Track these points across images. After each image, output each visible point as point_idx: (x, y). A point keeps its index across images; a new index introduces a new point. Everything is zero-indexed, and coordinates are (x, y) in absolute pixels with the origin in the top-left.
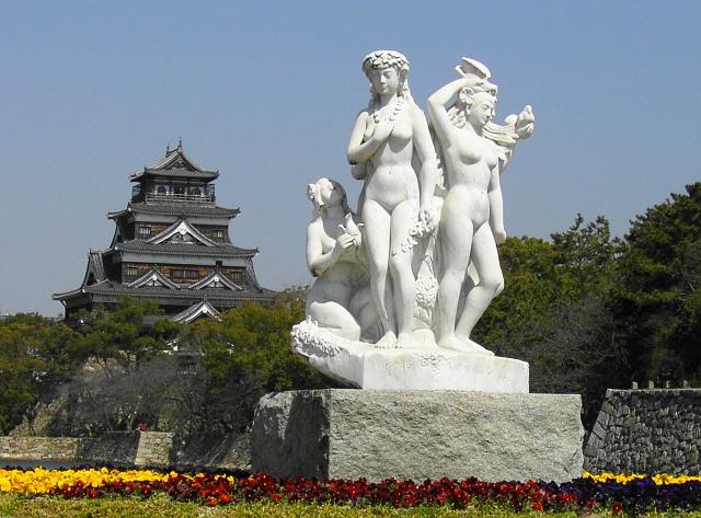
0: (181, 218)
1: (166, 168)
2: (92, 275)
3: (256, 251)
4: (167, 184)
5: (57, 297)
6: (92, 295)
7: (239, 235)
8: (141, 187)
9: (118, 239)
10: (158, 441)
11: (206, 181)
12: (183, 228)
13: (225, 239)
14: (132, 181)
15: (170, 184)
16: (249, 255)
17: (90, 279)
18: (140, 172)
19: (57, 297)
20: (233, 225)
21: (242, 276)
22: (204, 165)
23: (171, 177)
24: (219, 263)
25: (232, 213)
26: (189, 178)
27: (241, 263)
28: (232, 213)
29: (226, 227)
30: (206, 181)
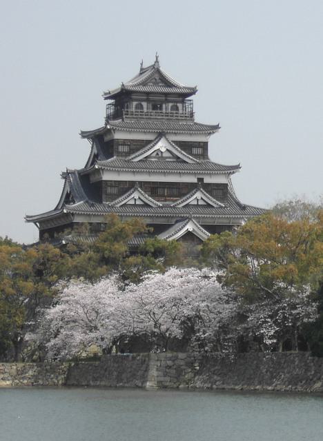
0: (161, 135)
1: (144, 84)
4: (144, 101)
6: (73, 214)
7: (217, 154)
8: (115, 105)
9: (94, 158)
10: (170, 363)
11: (184, 96)
12: (162, 145)
13: (204, 155)
14: (106, 99)
15: (148, 100)
18: (115, 87)
19: (29, 219)
20: (213, 141)
22: (180, 77)
23: (148, 94)
24: (201, 180)
26: (166, 94)
29: (204, 146)
30: (184, 96)
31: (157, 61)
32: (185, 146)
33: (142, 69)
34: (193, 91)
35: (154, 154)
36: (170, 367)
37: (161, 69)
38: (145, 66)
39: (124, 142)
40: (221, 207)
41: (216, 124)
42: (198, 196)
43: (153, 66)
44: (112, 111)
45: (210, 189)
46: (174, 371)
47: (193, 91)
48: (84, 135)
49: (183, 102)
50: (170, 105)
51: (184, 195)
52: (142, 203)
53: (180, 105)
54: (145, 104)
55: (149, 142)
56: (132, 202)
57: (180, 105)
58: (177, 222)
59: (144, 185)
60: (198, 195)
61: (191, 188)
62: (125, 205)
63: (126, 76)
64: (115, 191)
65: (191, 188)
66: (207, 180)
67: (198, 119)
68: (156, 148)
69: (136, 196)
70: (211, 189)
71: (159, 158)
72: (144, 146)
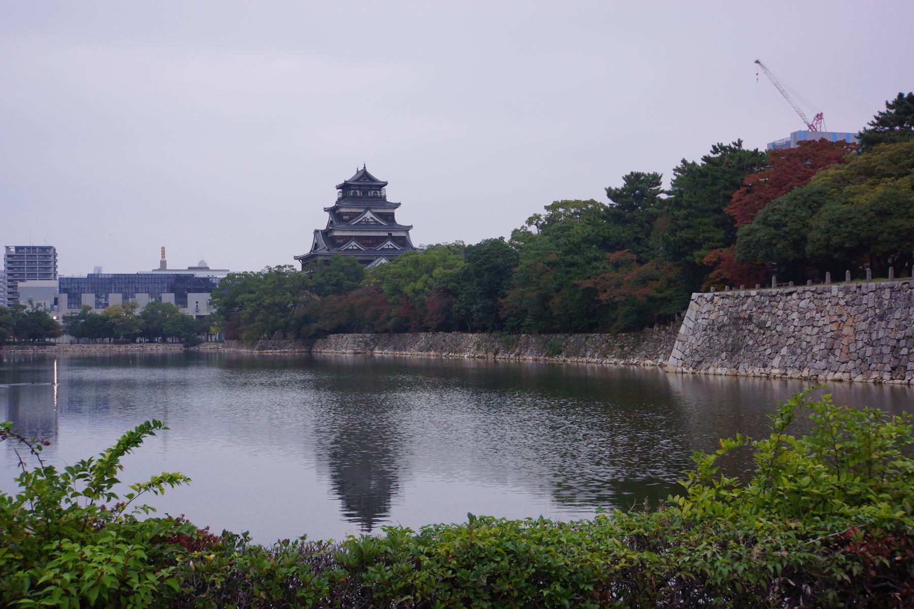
0: (367, 209)
1: (358, 180)
2: (316, 244)
3: (411, 227)
5: (296, 258)
7: (401, 218)
9: (331, 223)
10: (361, 339)
12: (369, 215)
13: (393, 220)
14: (337, 189)
16: (407, 229)
17: (316, 246)
19: (296, 258)
21: (404, 242)
23: (360, 186)
24: (390, 234)
25: (397, 205)
26: (370, 186)
27: (403, 234)
28: (397, 205)
29: (393, 214)
31: (365, 167)
32: (379, 215)
33: (357, 171)
34: (386, 184)
35: (363, 220)
36: (361, 342)
37: (367, 170)
38: (359, 170)
39: (346, 214)
40: (402, 250)
41: (398, 202)
42: (389, 244)
43: (363, 170)
44: (341, 195)
45: (394, 239)
46: (363, 344)
47: (386, 184)
48: (326, 210)
49: (380, 190)
50: (373, 192)
51: (382, 243)
52: (356, 248)
53: (378, 192)
54: (358, 192)
55: (361, 213)
56: (351, 248)
57: (378, 192)
58: (376, 258)
59: (358, 239)
60: (389, 243)
61: (384, 239)
62: (347, 249)
63: (349, 175)
64: (340, 241)
65: (384, 239)
66: (394, 234)
67: (388, 199)
68: (364, 216)
69: (353, 245)
70: (394, 239)
71: (366, 222)
72: (357, 216)
